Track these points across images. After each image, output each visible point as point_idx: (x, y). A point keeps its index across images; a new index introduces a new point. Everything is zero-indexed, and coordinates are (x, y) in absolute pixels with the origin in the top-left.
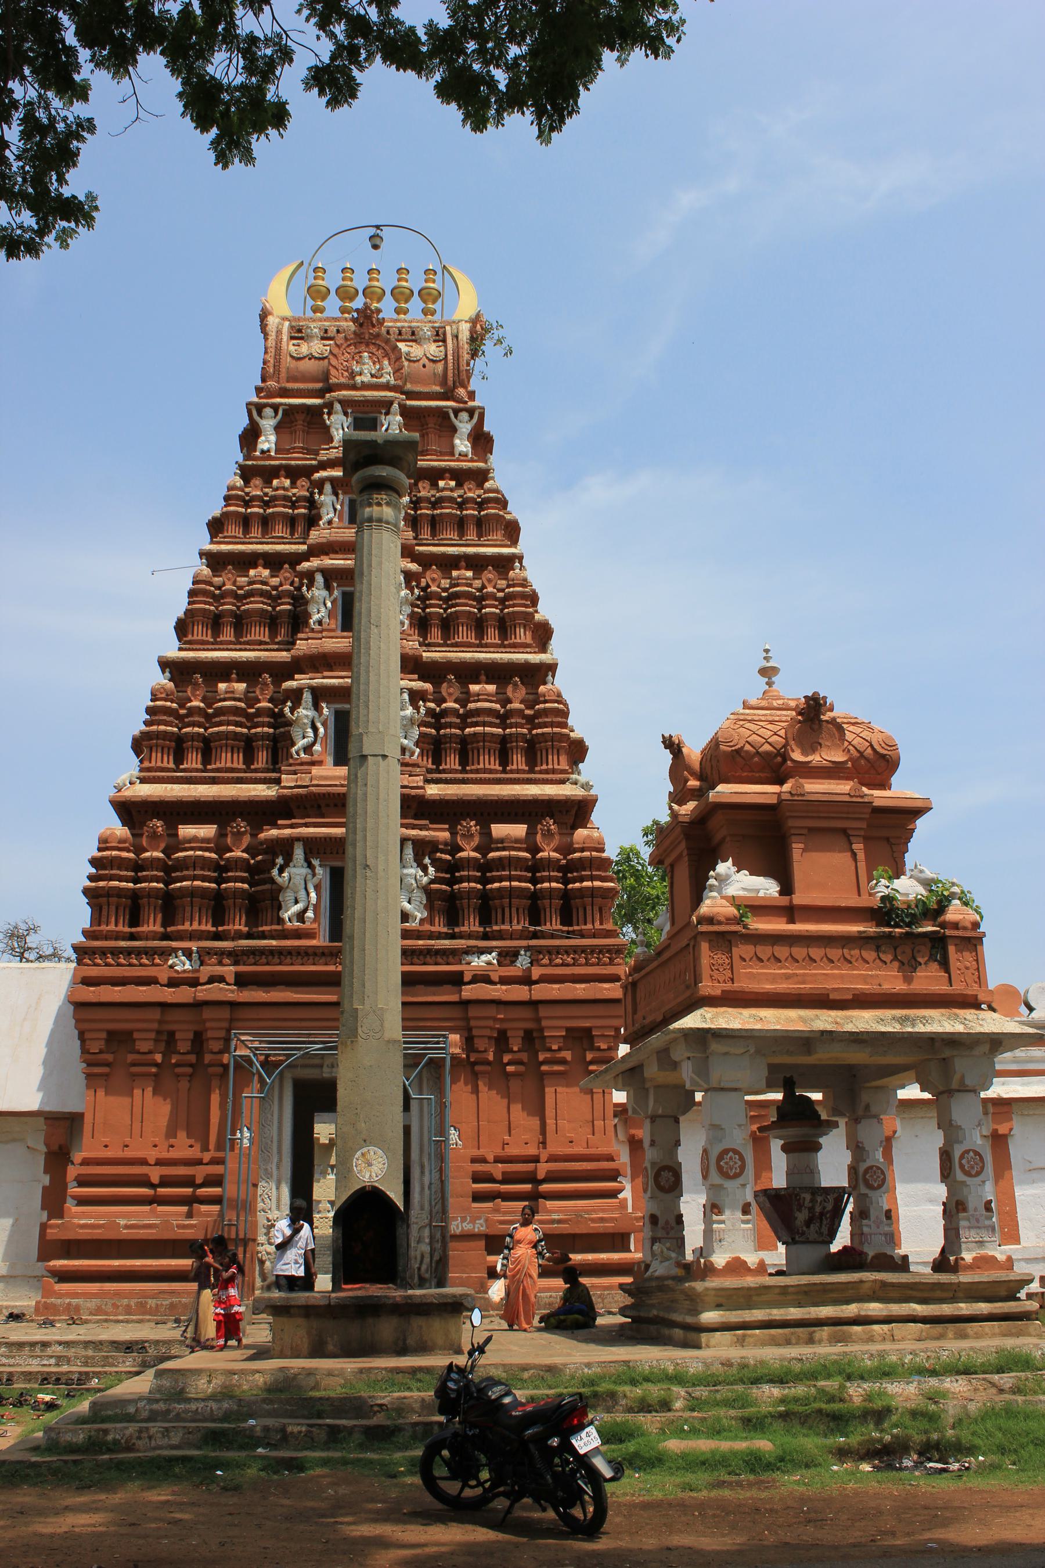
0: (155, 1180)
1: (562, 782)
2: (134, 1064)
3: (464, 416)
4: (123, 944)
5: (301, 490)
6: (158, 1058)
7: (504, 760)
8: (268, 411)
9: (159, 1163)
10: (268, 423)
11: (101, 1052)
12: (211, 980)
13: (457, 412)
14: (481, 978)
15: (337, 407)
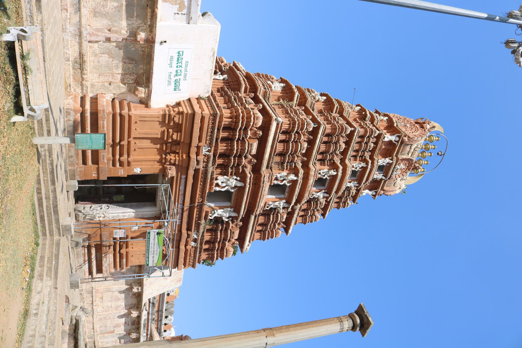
0: (122, 143)
1: (249, 242)
2: (168, 131)
3: (374, 194)
4: (216, 131)
5: (367, 155)
6: (170, 140)
7: (260, 225)
8: (397, 139)
9: (129, 142)
10: (393, 138)
11: (174, 122)
12: (198, 162)
13: (376, 192)
14: (188, 236)
15: (391, 162)
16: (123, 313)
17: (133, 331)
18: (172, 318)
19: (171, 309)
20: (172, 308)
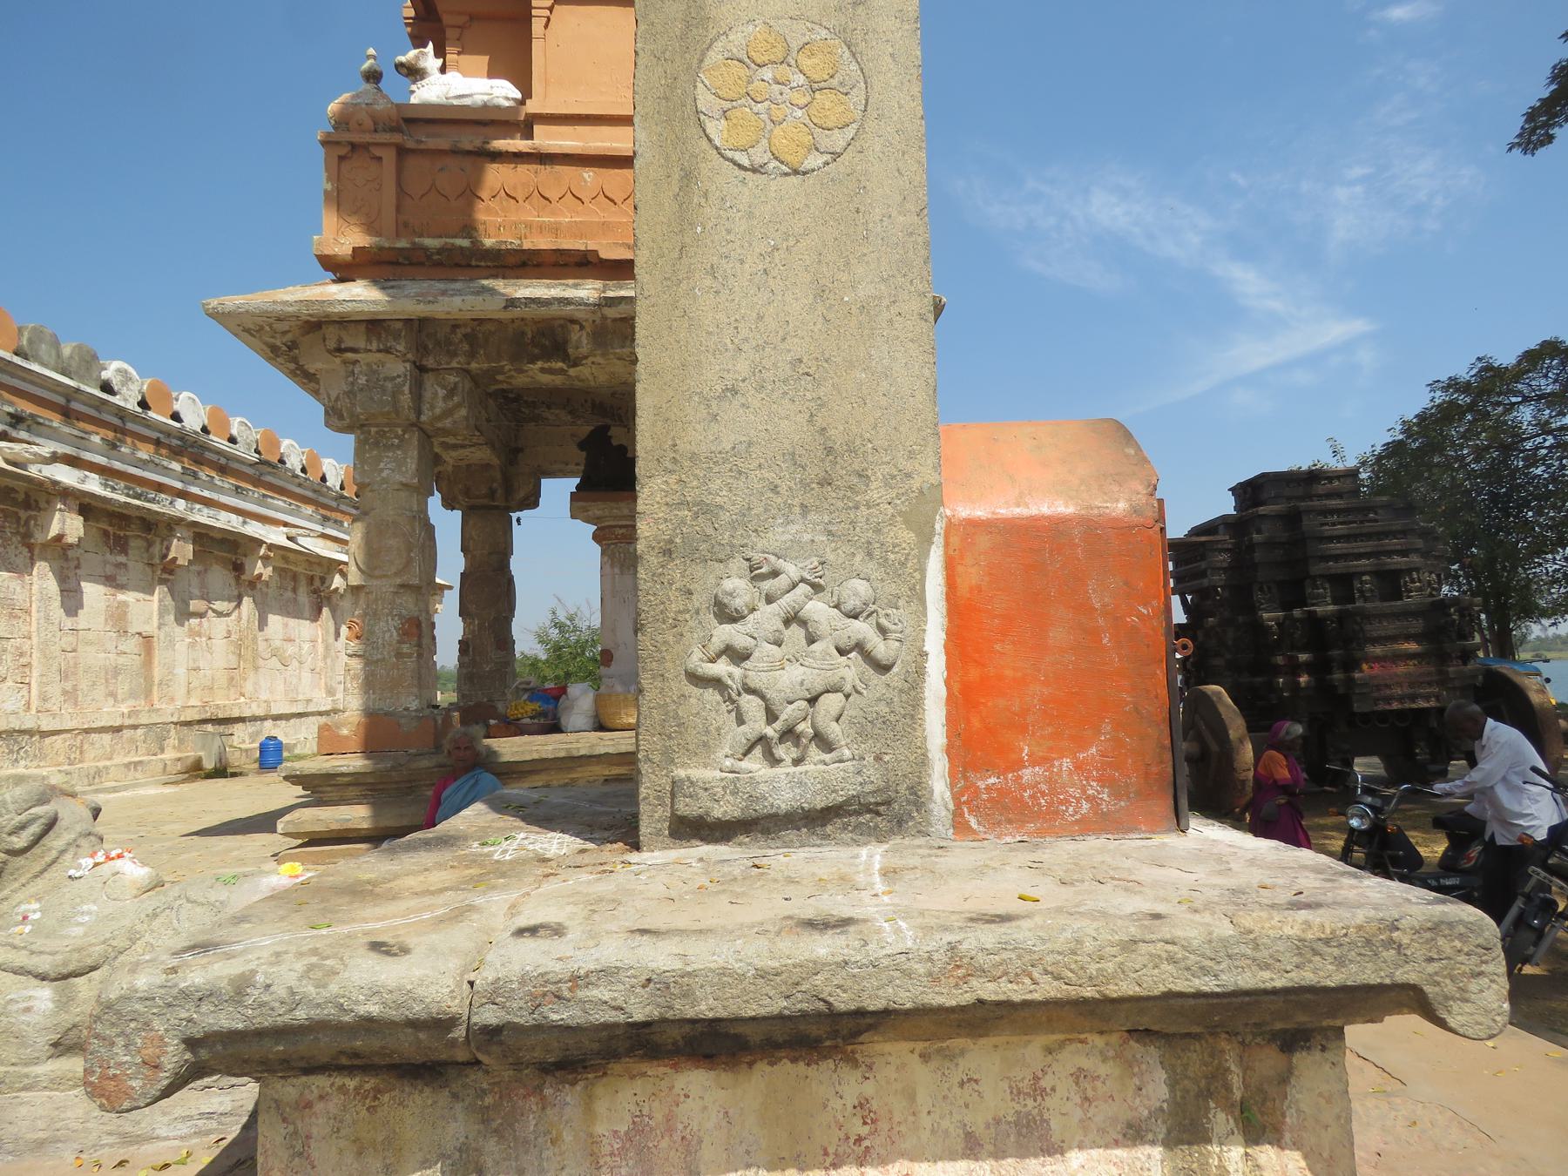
16: (52, 586)
17: (157, 549)
18: (116, 365)
19: (67, 351)
20: (56, 344)
